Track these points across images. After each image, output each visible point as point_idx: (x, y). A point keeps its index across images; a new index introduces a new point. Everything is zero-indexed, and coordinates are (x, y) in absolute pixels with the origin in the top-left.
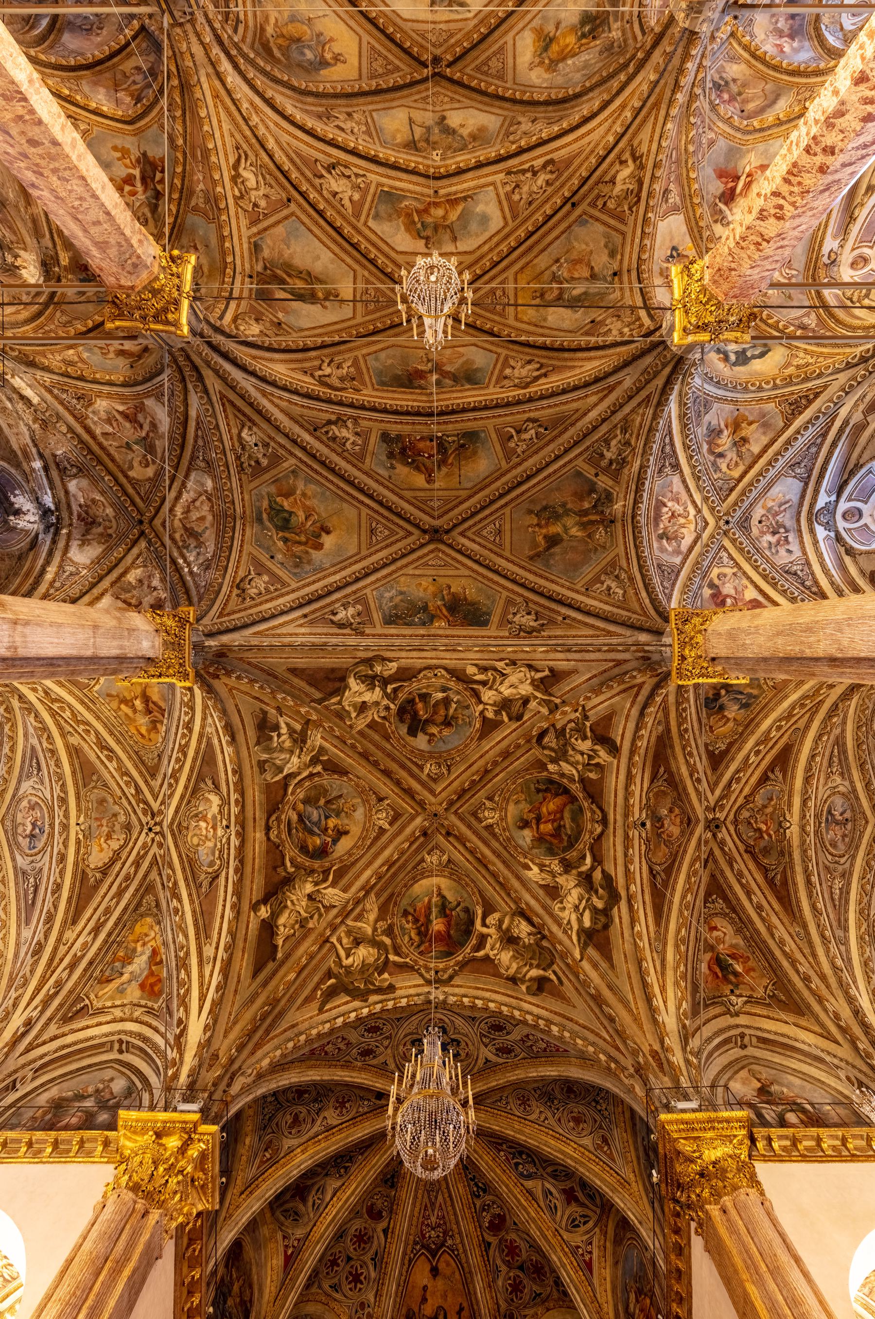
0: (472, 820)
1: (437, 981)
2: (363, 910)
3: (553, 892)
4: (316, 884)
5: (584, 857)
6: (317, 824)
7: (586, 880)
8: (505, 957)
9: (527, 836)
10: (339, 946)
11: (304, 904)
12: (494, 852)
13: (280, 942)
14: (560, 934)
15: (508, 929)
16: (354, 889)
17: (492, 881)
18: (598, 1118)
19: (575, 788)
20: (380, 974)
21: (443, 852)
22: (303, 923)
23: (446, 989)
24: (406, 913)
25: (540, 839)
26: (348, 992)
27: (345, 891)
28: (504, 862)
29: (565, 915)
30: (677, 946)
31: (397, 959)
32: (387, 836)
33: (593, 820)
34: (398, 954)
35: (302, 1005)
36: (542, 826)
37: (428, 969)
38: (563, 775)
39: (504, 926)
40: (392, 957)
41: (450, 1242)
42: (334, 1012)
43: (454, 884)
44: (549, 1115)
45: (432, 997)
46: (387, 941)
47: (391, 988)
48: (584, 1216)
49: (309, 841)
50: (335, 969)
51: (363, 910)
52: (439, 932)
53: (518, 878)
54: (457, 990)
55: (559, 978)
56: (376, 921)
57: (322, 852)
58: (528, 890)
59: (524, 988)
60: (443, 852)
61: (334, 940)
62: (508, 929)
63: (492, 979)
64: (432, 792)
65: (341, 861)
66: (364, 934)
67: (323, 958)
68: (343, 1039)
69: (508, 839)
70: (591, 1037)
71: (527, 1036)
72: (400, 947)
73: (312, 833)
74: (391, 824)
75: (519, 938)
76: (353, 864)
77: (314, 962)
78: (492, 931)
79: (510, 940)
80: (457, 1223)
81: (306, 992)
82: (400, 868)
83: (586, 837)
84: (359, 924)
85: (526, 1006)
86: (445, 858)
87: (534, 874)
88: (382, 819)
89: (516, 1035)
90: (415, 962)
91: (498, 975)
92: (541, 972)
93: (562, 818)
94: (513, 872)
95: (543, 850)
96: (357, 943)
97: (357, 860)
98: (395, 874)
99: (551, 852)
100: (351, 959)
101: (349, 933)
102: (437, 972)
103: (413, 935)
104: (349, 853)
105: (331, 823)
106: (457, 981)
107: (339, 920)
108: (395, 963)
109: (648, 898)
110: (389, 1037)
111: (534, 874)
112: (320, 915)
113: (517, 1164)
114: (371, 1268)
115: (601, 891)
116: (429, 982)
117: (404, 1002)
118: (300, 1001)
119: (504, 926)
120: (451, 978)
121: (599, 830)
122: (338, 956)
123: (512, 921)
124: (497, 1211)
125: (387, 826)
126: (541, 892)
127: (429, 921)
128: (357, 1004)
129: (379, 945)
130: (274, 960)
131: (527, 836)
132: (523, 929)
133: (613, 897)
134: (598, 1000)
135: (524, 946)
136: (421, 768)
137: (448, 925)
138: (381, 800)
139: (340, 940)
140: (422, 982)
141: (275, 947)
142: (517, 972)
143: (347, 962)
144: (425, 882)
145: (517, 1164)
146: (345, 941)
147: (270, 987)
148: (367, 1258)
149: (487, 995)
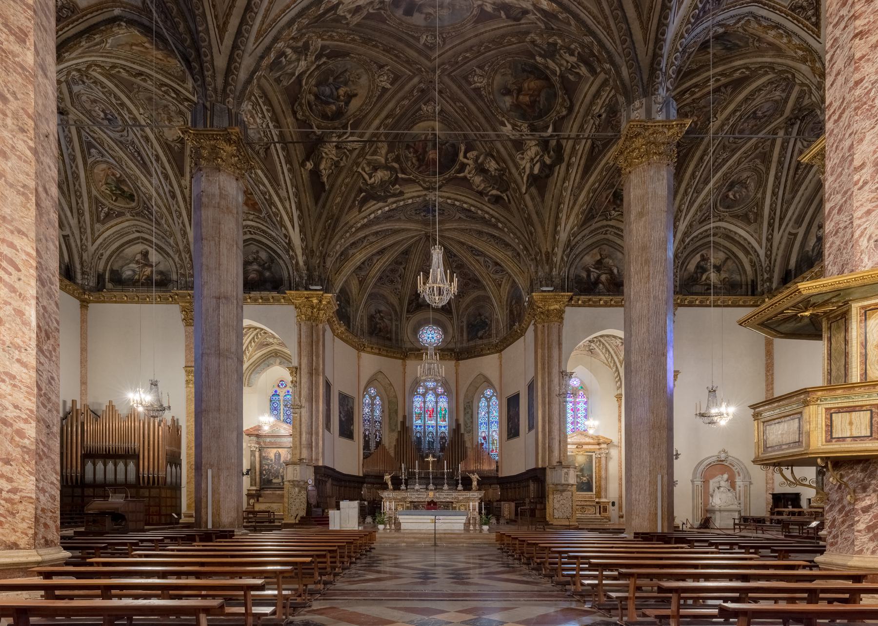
2: (377, 147)
3: (519, 145)
5: (547, 127)
6: (331, 96)
7: (544, 144)
8: (478, 180)
9: (508, 101)
10: (364, 173)
13: (325, 180)
14: (516, 175)
19: (555, 79)
22: (336, 164)
24: (408, 147)
25: (517, 106)
26: (374, 199)
28: (486, 118)
30: (588, 193)
33: (562, 105)
35: (348, 211)
37: (425, 182)
38: (548, 68)
40: (400, 175)
42: (368, 211)
46: (396, 165)
49: (327, 110)
51: (377, 147)
55: (509, 200)
56: (387, 154)
57: (339, 114)
62: (482, 163)
64: (428, 58)
70: (519, 234)
73: (328, 103)
74: (392, 84)
75: (488, 170)
78: (470, 162)
79: (481, 170)
81: (349, 204)
83: (553, 115)
84: (375, 157)
85: (486, 208)
87: (507, 129)
88: (384, 81)
90: (416, 177)
92: (499, 193)
93: (539, 95)
96: (375, 169)
99: (524, 117)
100: (373, 179)
101: (369, 164)
104: (360, 109)
105: (341, 91)
109: (584, 157)
111: (507, 129)
112: (347, 157)
115: (552, 153)
117: (410, 201)
118: (346, 210)
119: (479, 161)
121: (564, 113)
122: (364, 179)
123: (485, 159)
125: (389, 86)
126: (509, 144)
128: (381, 204)
129: (392, 169)
130: (325, 191)
131: (508, 101)
132: (492, 165)
133: (559, 159)
134: (529, 221)
136: (418, 39)
138: (381, 67)
139: (363, 169)
140: (421, 189)
141: (323, 183)
143: (370, 182)
144: (422, 124)
146: (367, 169)
147: (327, 207)
149: (463, 198)
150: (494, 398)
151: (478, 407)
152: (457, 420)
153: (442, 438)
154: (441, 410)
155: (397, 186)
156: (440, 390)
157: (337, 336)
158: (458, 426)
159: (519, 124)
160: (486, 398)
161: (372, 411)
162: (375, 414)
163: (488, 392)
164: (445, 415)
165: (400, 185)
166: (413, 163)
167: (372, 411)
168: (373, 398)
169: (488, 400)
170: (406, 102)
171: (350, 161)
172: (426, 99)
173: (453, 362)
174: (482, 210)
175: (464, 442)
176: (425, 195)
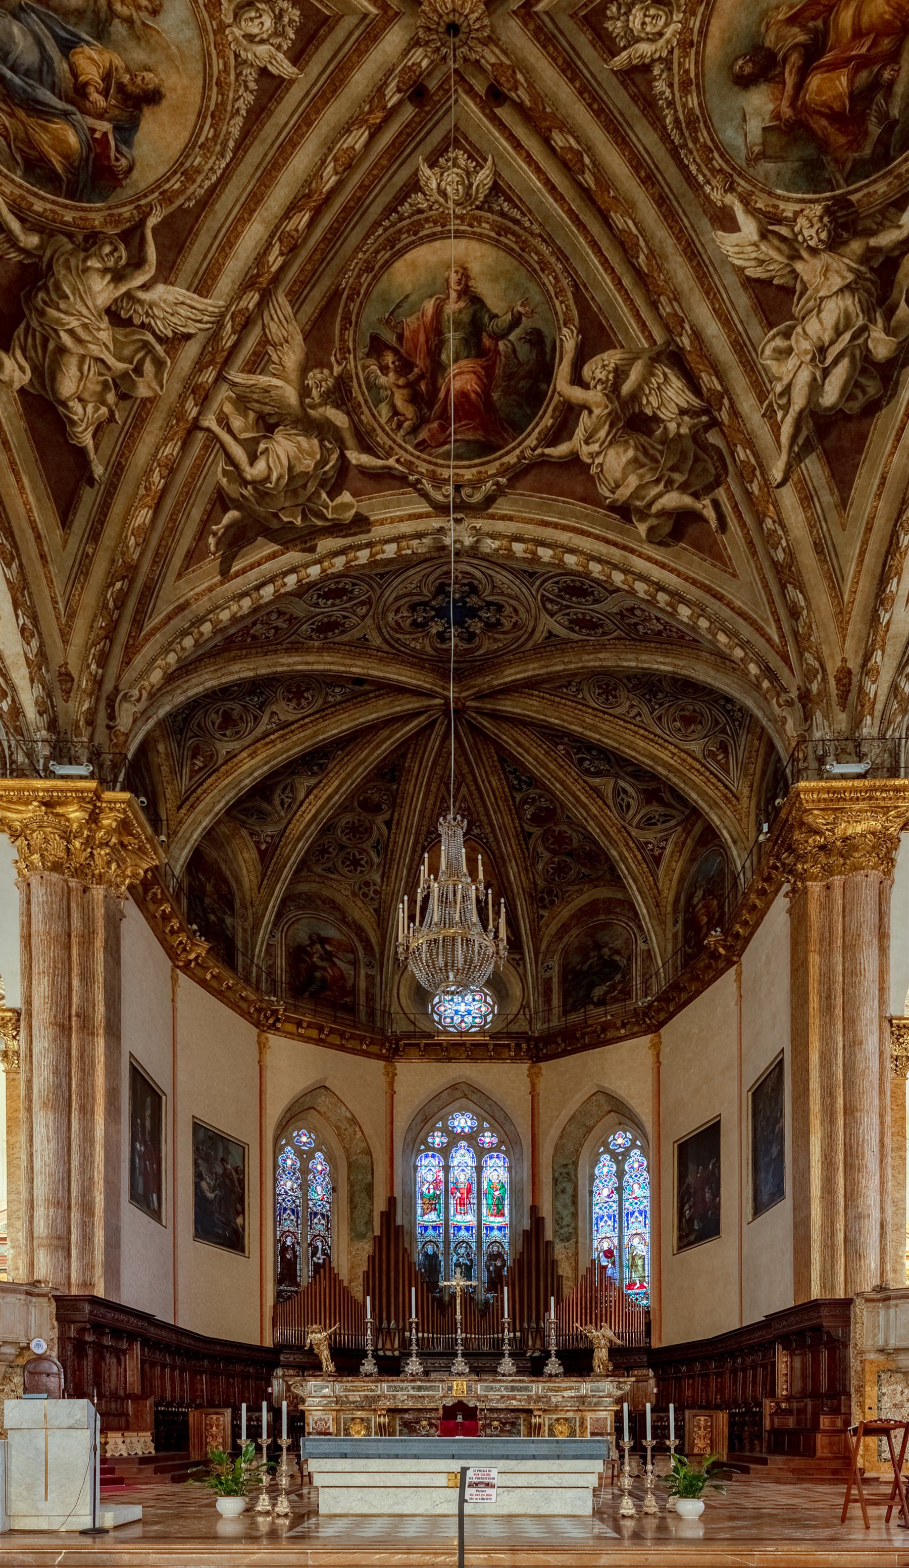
0: (583, 41)
1: (461, 506)
2: (265, 341)
4: (118, 276)
11: (105, 335)
12: (637, 163)
15: (635, 396)
16: (226, 283)
17: (614, 259)
20: (332, 495)
21: (477, 156)
23: (479, 523)
27: (203, 287)
28: (661, 201)
29: (784, 370)
31: (366, 459)
32: (295, 94)
34: (367, 448)
36: (815, 81)
37: (439, 482)
39: (626, 388)
40: (355, 457)
43: (508, 262)
45: (448, 541)
46: (339, 418)
47: (361, 523)
50: (233, 490)
51: (265, 341)
52: (463, 395)
53: (692, 253)
54: (500, 526)
56: (304, 370)
58: (710, 292)
59: (642, 529)
60: (477, 156)
61: (210, 421)
63: (579, 507)
65: (167, 198)
66: (281, 403)
67: (198, 467)
68: (280, 613)
69: (692, 121)
71: (632, 610)
72: (371, 432)
75: (656, 419)
76: (206, 202)
77: (181, 478)
78: (594, 396)
80: (488, 814)
82: (347, 211)
84: (263, 380)
85: (640, 564)
86: (483, 177)
89: (610, 605)
90: (409, 465)
91: (593, 499)
94: (680, 234)
95: (787, 168)
97: (213, 192)
98: (335, 234)
101: (242, 402)
102: (458, 488)
103: (399, 403)
106: (502, 507)
107: (208, 376)
108: (363, 470)
110: (368, 602)
112: (159, 364)
116: (442, 509)
117: (390, 550)
119: (626, 388)
120: (490, 500)
122: (230, 459)
123: (649, 373)
126: (742, 300)
127: (437, 368)
135: (664, 441)
137: (487, 377)
142: (635, 495)
146: (237, 423)
149: (564, 537)
152: (534, 1209)
153: (493, 1257)
154: (492, 1187)
155: (346, 497)
157: (186, 969)
158: (537, 1222)
159: (788, 208)
165: (354, 495)
166: (395, 412)
170: (358, 139)
171: (173, 387)
172: (436, 137)
174: (625, 571)
175: (554, 1263)
176: (441, 530)
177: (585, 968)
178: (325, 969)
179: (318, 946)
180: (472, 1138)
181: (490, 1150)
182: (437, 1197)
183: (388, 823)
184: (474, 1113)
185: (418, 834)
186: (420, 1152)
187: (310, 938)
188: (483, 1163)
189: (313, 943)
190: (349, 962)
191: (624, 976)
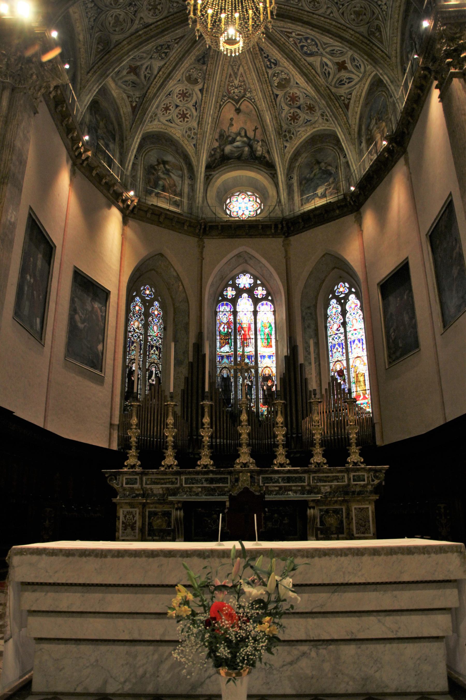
18: (376, 12)
41: (248, 95)
44: (335, 9)
48: (349, 78)
113: (302, 47)
114: (194, 110)
124: (284, 76)
145: (302, 47)
148: (190, 105)
150: (352, 297)
151: (326, 317)
156: (260, 292)
160: (339, 300)
161: (146, 326)
162: (150, 333)
163: (342, 288)
164: (269, 335)
167: (146, 326)
168: (147, 304)
169: (343, 302)
173: (280, 240)
177: (312, 176)
178: (165, 179)
179: (162, 166)
180: (250, 291)
181: (262, 299)
182: (230, 333)
183: (201, 91)
184: (251, 275)
185: (218, 97)
186: (219, 302)
187: (158, 161)
188: (258, 309)
189: (159, 164)
190: (179, 176)
191: (335, 179)
